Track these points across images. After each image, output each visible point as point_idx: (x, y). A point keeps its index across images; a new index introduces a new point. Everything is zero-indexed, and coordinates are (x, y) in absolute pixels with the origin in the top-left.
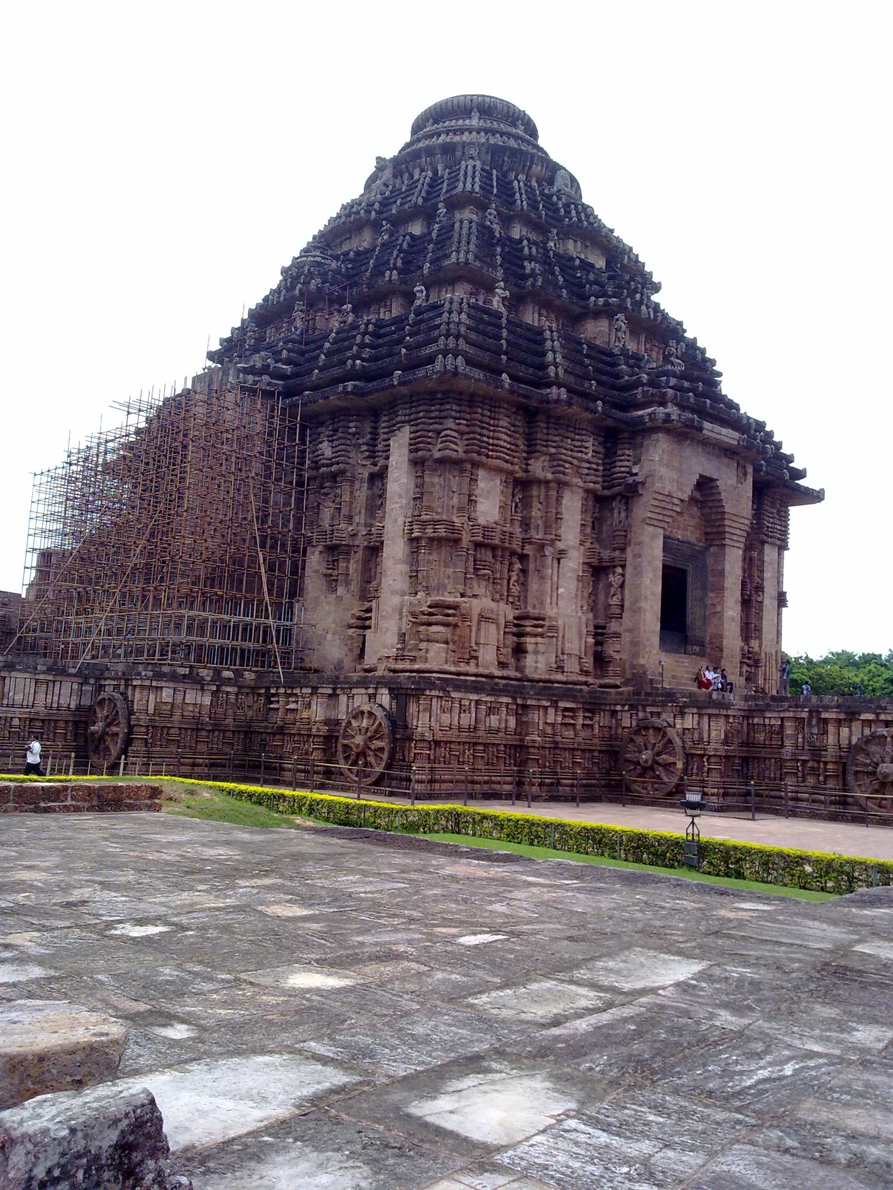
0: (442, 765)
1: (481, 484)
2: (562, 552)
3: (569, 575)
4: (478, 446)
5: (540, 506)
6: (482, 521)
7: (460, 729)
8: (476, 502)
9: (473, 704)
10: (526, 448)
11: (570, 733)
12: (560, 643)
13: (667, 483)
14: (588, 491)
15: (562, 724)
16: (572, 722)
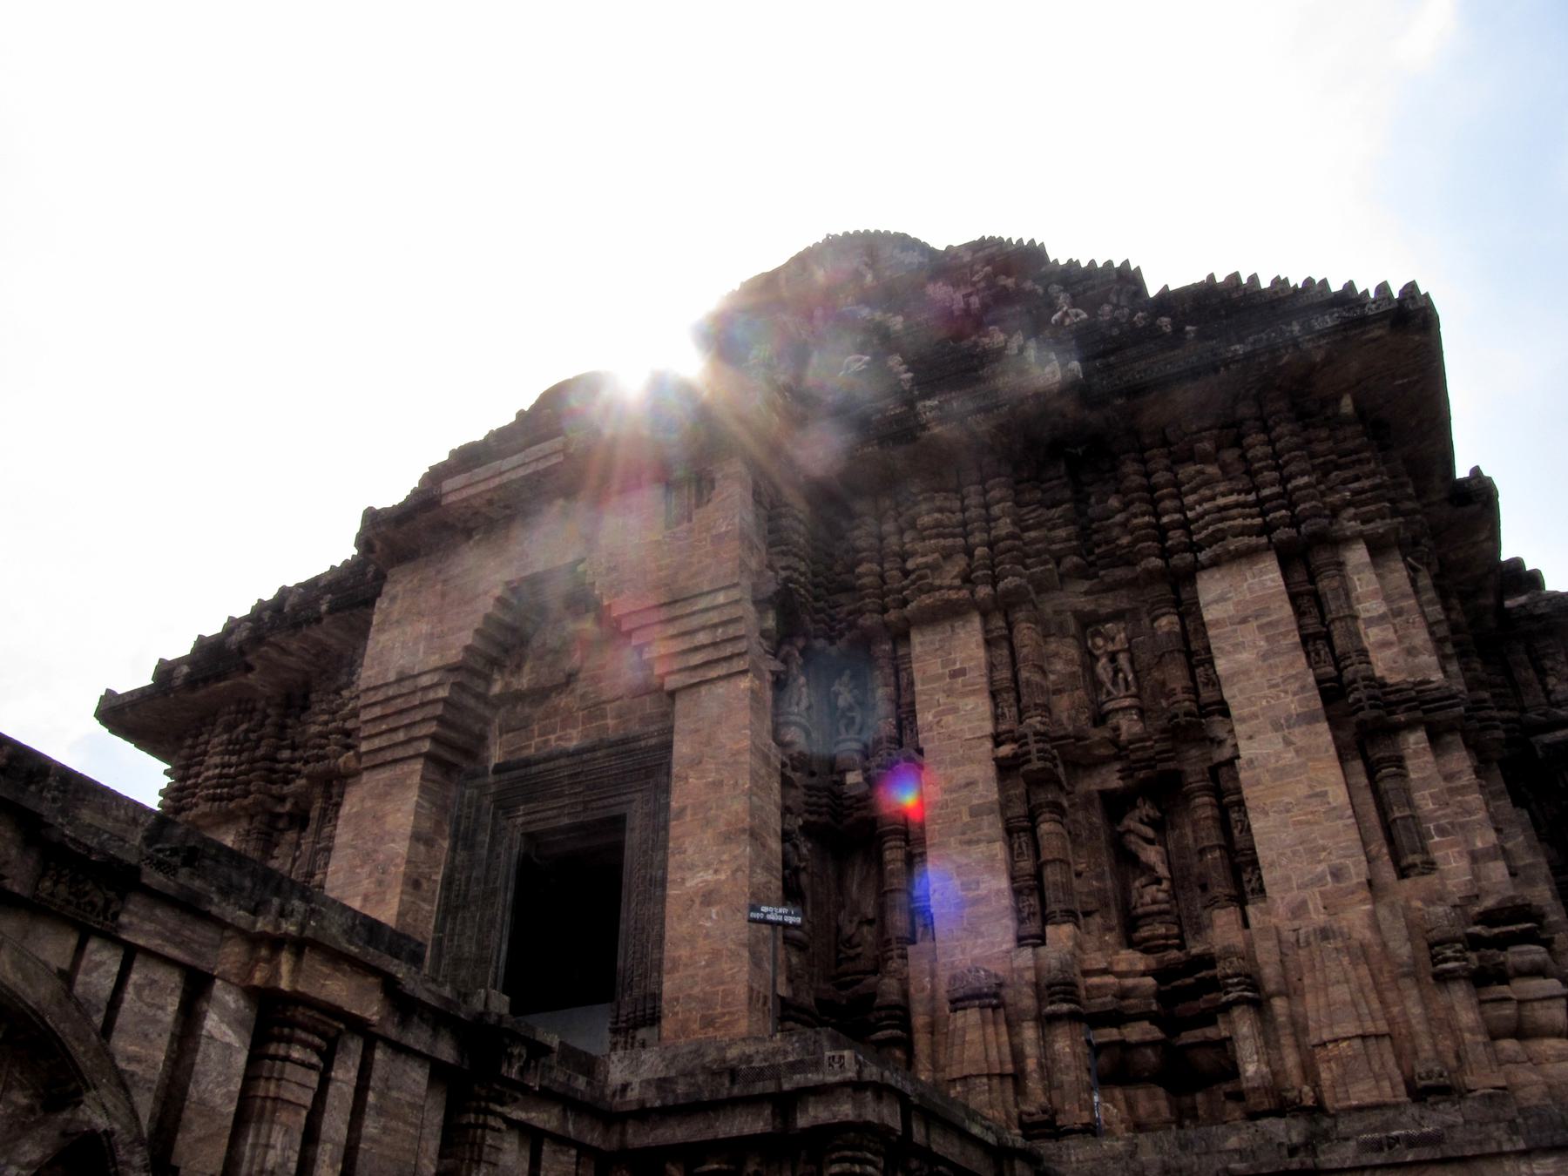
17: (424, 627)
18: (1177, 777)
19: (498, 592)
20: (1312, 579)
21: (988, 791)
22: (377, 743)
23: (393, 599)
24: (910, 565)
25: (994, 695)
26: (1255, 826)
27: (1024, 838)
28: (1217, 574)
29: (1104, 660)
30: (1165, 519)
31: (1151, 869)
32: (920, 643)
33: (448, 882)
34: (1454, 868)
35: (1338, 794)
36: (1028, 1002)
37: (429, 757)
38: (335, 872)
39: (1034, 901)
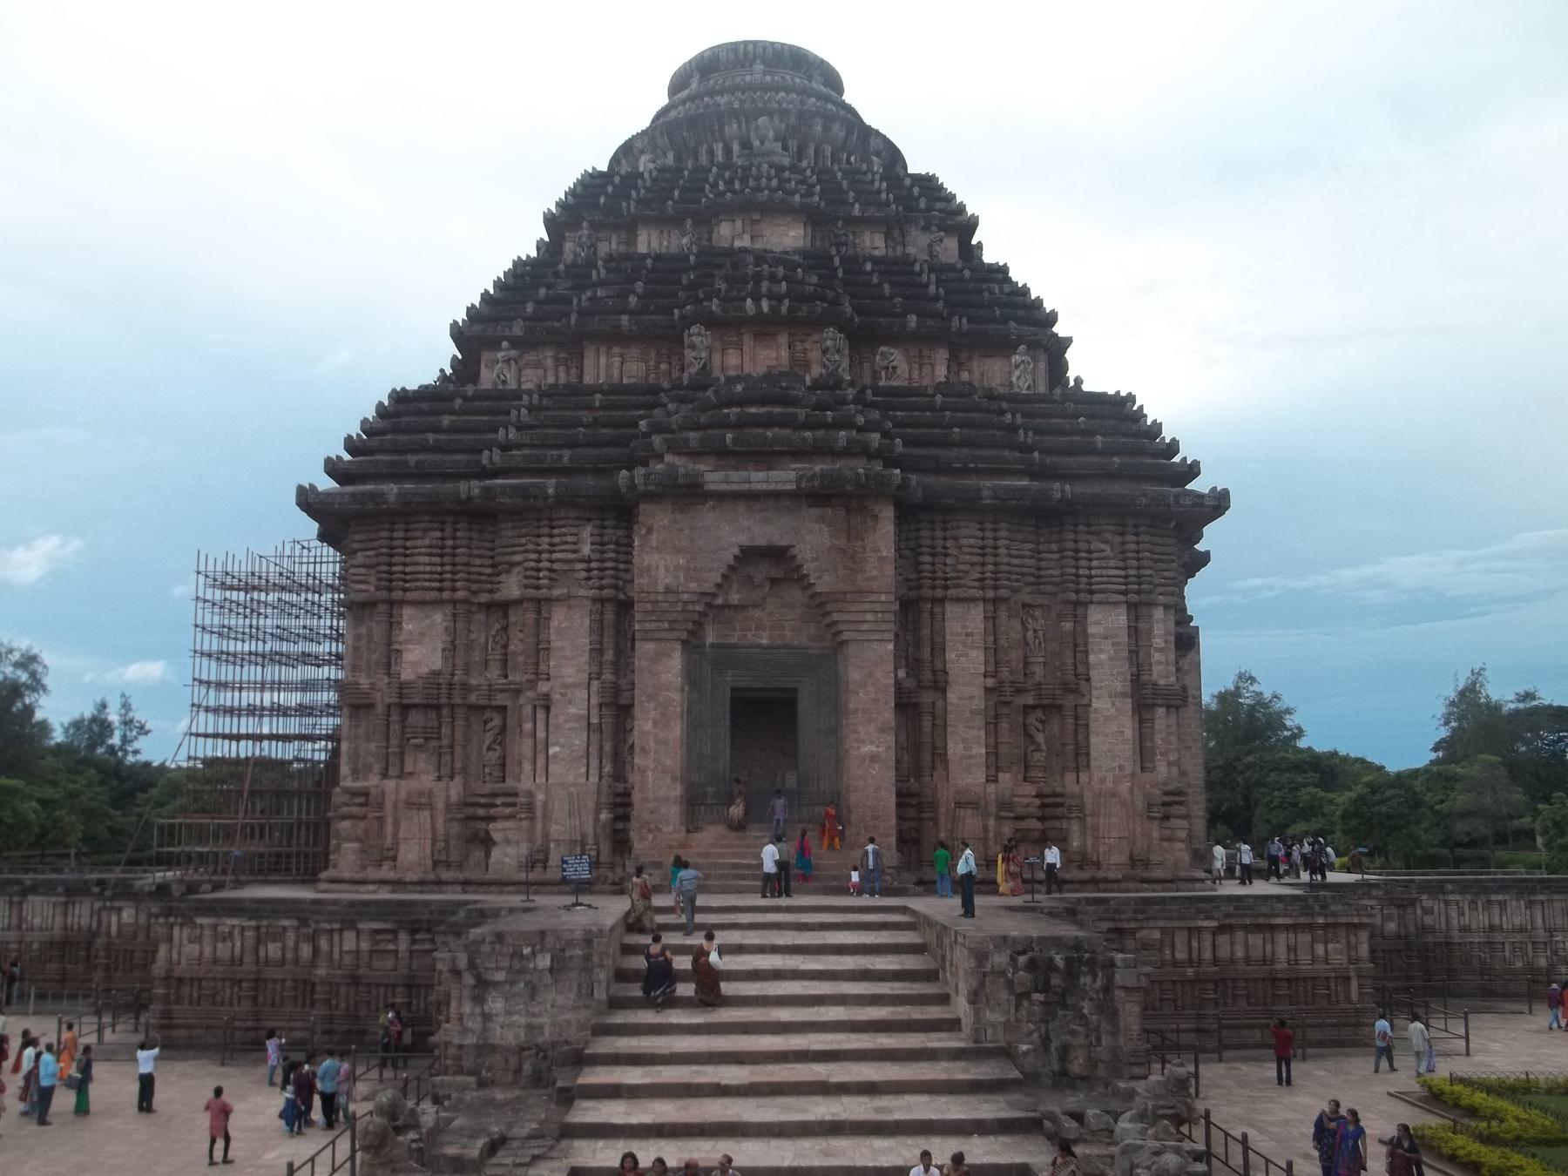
0: (186, 1006)
1: (408, 626)
2: (547, 696)
3: (568, 725)
4: (387, 580)
5: (521, 636)
6: (404, 677)
7: (215, 961)
8: (398, 651)
9: (236, 932)
10: (490, 562)
11: (390, 963)
12: (539, 826)
13: (662, 573)
14: (594, 600)
15: (371, 952)
16: (391, 947)
17: (681, 561)
18: (1059, 708)
19: (736, 551)
20: (1137, 620)
21: (979, 704)
22: (648, 626)
23: (650, 530)
24: (949, 561)
25: (986, 649)
26: (1093, 740)
27: (992, 727)
28: (1099, 608)
29: (1030, 633)
30: (1081, 572)
31: (1039, 745)
32: (951, 609)
33: (689, 711)
34: (1162, 770)
35: (1129, 734)
36: (993, 810)
37: (685, 643)
38: (555, 667)
39: (993, 758)
